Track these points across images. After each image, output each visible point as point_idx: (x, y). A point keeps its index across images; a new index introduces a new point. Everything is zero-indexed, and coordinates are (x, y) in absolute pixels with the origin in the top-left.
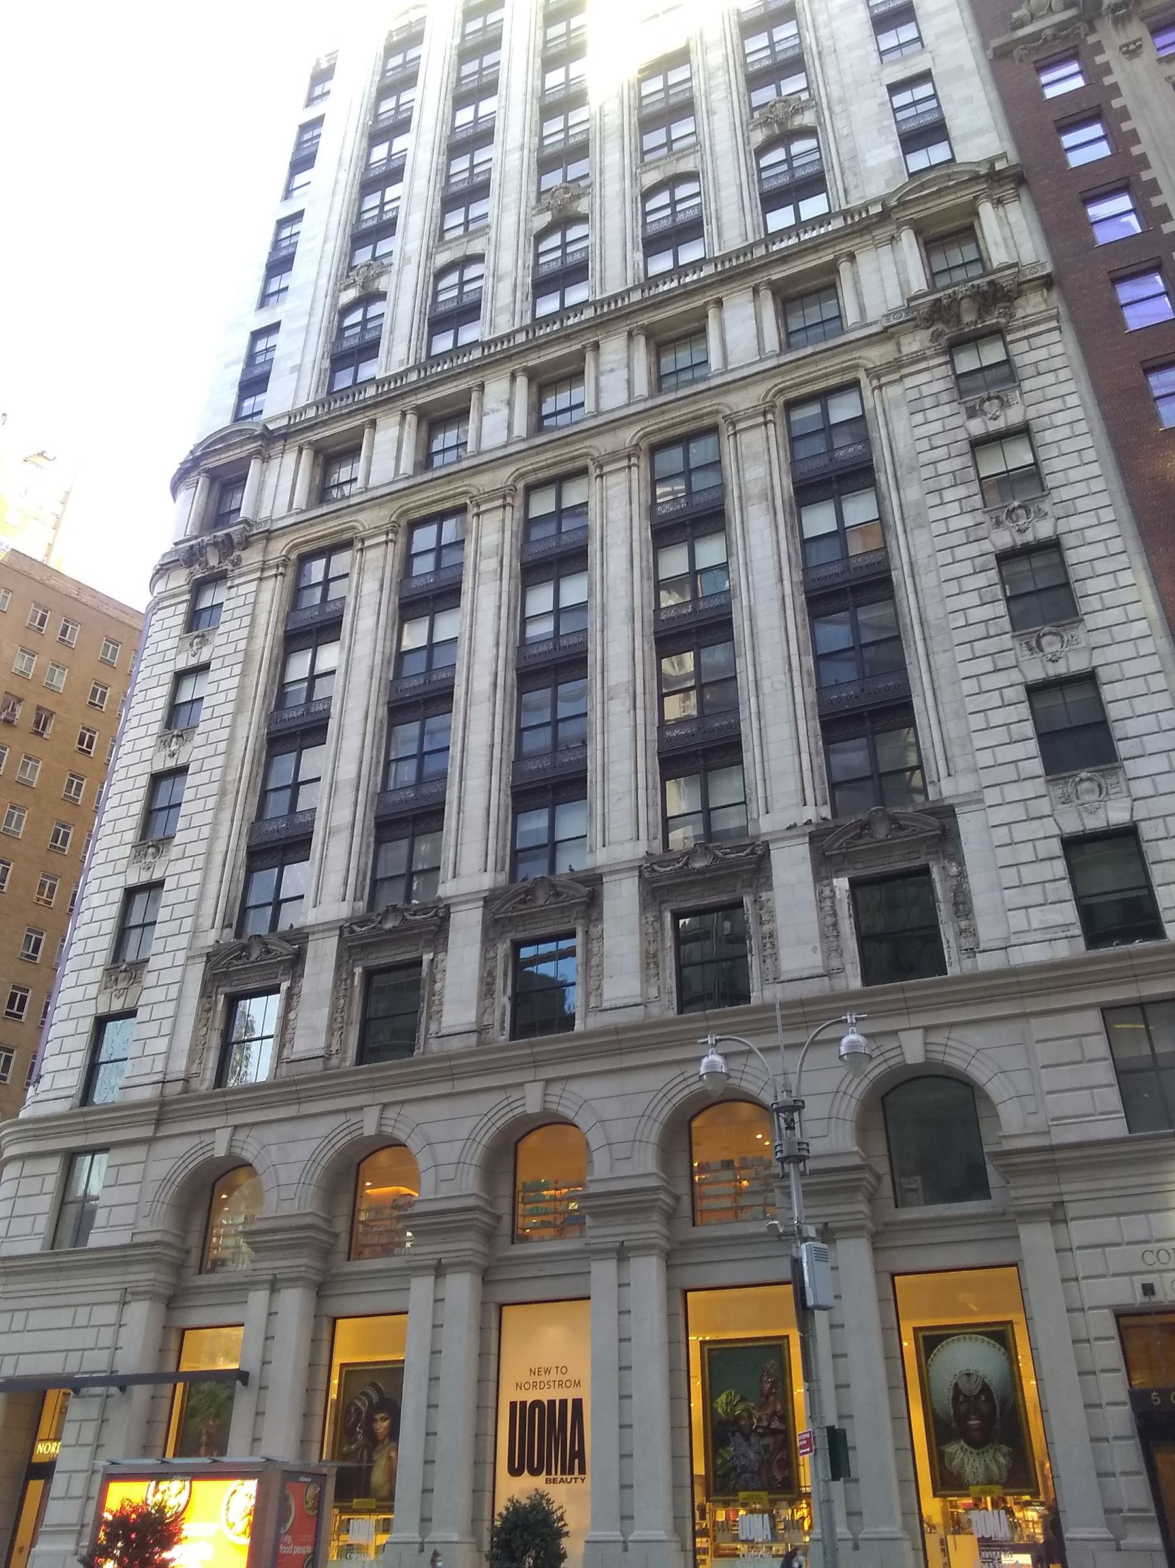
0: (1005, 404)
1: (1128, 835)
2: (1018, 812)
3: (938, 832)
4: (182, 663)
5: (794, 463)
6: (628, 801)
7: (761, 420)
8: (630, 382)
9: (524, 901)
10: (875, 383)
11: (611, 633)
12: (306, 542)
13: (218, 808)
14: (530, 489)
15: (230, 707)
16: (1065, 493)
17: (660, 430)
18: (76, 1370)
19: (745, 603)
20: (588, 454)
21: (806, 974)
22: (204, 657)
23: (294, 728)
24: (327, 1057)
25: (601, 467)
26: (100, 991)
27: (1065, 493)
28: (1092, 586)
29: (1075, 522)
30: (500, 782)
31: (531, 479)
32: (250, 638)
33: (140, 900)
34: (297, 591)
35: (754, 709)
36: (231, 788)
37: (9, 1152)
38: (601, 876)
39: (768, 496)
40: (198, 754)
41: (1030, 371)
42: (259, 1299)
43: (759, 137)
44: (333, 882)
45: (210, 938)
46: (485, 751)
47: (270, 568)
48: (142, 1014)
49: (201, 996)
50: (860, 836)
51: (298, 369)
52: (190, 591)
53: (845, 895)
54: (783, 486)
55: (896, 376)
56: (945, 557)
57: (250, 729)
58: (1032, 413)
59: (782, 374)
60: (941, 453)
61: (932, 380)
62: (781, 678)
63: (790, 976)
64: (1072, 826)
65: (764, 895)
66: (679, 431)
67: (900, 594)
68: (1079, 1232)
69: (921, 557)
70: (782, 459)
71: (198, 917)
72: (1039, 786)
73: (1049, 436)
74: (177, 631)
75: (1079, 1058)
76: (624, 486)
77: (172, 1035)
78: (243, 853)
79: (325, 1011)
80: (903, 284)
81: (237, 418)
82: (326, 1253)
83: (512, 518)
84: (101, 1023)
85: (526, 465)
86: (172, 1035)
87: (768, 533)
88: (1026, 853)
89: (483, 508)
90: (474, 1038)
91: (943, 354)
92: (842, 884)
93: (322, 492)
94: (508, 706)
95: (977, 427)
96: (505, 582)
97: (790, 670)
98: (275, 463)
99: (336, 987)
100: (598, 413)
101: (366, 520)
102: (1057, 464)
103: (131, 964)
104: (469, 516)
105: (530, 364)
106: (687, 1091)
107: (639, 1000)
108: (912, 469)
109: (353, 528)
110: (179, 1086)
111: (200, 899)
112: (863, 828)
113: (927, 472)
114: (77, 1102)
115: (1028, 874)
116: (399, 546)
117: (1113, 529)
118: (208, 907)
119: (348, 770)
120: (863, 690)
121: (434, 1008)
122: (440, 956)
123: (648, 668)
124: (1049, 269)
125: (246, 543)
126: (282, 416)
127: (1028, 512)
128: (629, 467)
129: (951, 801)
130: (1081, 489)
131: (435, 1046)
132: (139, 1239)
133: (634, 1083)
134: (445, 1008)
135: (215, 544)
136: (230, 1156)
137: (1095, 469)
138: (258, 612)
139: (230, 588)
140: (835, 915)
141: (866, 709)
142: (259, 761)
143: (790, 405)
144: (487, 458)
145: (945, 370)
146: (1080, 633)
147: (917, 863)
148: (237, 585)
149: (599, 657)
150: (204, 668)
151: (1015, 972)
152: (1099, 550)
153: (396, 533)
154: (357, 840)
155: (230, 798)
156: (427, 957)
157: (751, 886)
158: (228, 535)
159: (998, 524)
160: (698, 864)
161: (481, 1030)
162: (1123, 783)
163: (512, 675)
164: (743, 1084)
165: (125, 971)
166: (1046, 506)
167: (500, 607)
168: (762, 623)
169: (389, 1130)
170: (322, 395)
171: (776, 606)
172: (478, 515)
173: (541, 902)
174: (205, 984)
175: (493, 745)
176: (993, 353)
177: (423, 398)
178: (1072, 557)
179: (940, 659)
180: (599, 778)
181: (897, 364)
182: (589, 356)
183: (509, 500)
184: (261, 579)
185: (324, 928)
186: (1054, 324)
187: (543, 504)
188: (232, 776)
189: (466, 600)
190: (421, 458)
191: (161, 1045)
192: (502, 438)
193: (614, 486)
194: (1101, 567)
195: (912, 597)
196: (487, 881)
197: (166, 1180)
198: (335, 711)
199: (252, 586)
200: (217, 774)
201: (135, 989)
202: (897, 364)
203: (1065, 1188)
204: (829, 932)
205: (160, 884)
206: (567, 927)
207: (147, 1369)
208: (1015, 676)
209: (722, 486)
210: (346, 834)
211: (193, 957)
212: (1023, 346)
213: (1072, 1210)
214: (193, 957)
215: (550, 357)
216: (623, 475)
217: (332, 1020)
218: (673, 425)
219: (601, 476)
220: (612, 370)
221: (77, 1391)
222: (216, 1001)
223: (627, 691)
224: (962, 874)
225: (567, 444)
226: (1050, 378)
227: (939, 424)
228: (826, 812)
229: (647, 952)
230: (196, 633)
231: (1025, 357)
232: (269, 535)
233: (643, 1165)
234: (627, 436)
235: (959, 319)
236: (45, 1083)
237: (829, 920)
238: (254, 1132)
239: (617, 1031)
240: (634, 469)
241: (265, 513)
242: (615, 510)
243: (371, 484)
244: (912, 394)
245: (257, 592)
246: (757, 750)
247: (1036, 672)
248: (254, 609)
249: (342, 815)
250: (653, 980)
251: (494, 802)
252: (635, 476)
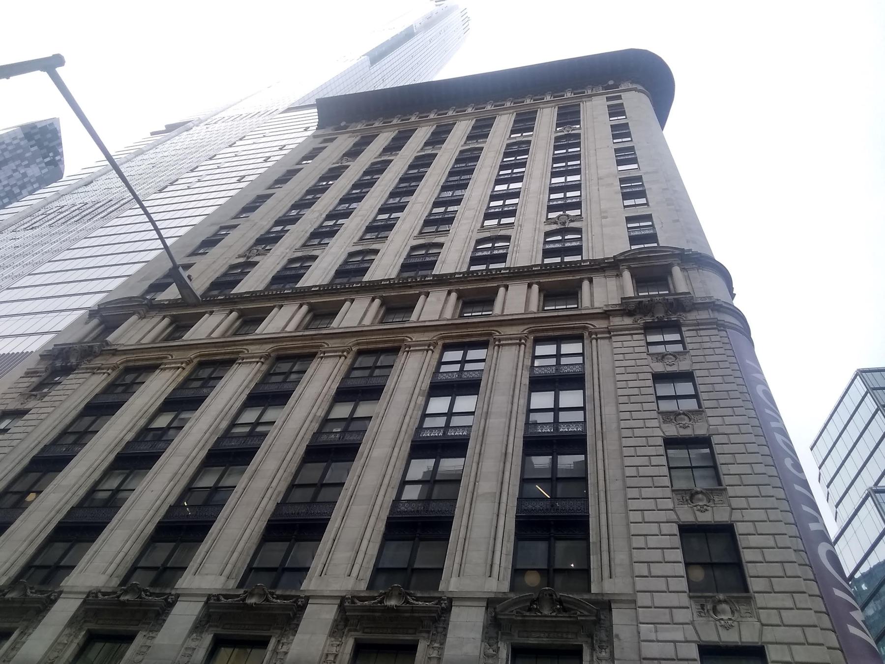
3: (594, 618)
100: (418, 321)
112: (533, 602)
120: (552, 506)
129: (611, 598)
157: (428, 632)
160: (392, 603)
172: (322, 358)
182: (422, 297)
228: (505, 587)
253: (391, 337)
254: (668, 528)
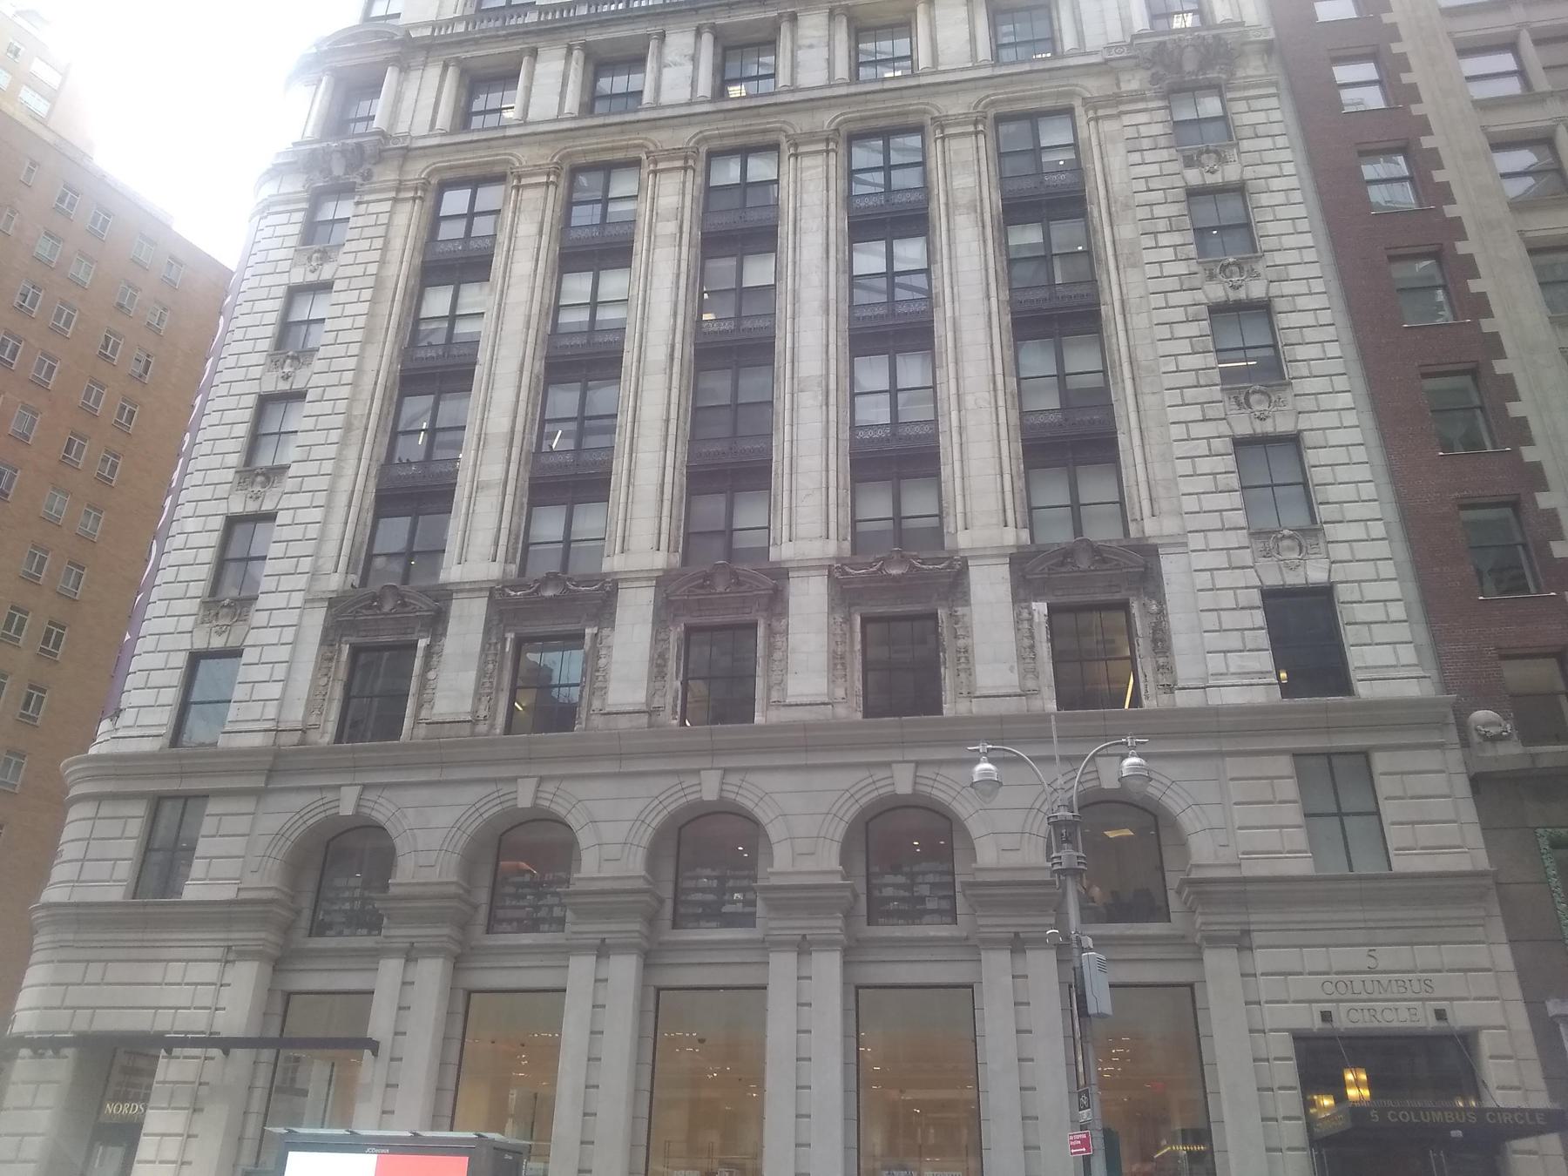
0: (1222, 160)
1: (1324, 594)
2: (1220, 560)
4: (299, 276)
5: (1002, 179)
6: (818, 498)
7: (971, 128)
8: (830, 63)
9: (702, 587)
10: (1091, 114)
11: (802, 321)
12: (451, 168)
13: (343, 443)
14: (712, 155)
15: (357, 336)
16: (1279, 258)
17: (862, 119)
18: (168, 1028)
19: (949, 314)
20: (781, 130)
21: (1002, 692)
22: (326, 273)
23: (434, 369)
24: (474, 722)
25: (796, 145)
26: (196, 625)
27: (1279, 258)
28: (1301, 352)
29: (1288, 288)
30: (676, 456)
31: (715, 144)
32: (382, 262)
33: (239, 530)
34: (436, 220)
35: (955, 423)
36: (358, 424)
37: (74, 792)
38: (787, 570)
39: (976, 207)
40: (316, 380)
41: (1248, 132)
42: (391, 969)
44: (482, 539)
45: (334, 582)
46: (660, 424)
47: (407, 189)
48: (249, 655)
49: (321, 644)
50: (1062, 564)
52: (308, 200)
53: (1044, 619)
54: (992, 200)
55: (1113, 111)
56: (1158, 301)
57: (380, 362)
58: (1249, 173)
59: (996, 87)
60: (1158, 196)
61: (1149, 122)
62: (985, 396)
63: (986, 692)
64: (1273, 579)
65: (960, 611)
66: (882, 123)
67: (1108, 330)
68: (1262, 959)
69: (1133, 295)
70: (992, 173)
71: (318, 558)
72: (1241, 538)
73: (1265, 199)
74: (293, 241)
75: (1270, 798)
76: (821, 170)
77: (286, 681)
78: (371, 496)
79: (472, 675)
80: (1125, 21)
81: (367, 18)
82: (464, 926)
83: (693, 183)
84: (196, 658)
85: (711, 129)
86: (286, 681)
87: (975, 246)
88: (1227, 600)
89: (661, 166)
90: (644, 719)
91: (1163, 98)
92: (1040, 608)
93: (464, 118)
94: (685, 382)
95: (1194, 177)
96: (685, 249)
97: (995, 390)
98: (415, 75)
99: (483, 649)
101: (524, 156)
102: (1272, 228)
103: (235, 600)
104: (644, 172)
105: (719, 22)
106: (875, 794)
107: (826, 700)
108: (1127, 206)
109: (508, 162)
110: (296, 737)
111: (320, 540)
113: (1142, 213)
114: (165, 741)
115: (1229, 620)
116: (560, 190)
117: (1322, 301)
118: (330, 548)
119: (499, 422)
121: (598, 685)
122: (606, 632)
123: (841, 366)
124: (1271, 35)
125: (380, 157)
126: (425, 25)
127: (1241, 269)
128: (828, 152)
130: (1293, 256)
131: (598, 721)
132: (244, 895)
133: (819, 780)
134: (612, 686)
135: (343, 152)
136: (357, 814)
137: (1308, 240)
138: (392, 234)
139: (358, 203)
140: (1032, 637)
141: (1070, 439)
142: (391, 398)
143: (1000, 119)
144: (669, 113)
145: (1161, 115)
146: (1287, 395)
147: (1117, 597)
148: (368, 202)
149: (789, 345)
150: (327, 286)
151: (1217, 711)
152: (1308, 319)
153: (558, 176)
154: (509, 499)
155: (356, 435)
156: (588, 631)
158: (359, 146)
159: (1211, 277)
161: (651, 712)
162: (1322, 545)
163: (690, 350)
164: (935, 792)
165: (229, 606)
166: (1259, 267)
167: (678, 276)
168: (966, 337)
169: (547, 804)
170: (471, 11)
171: (981, 322)
173: (720, 589)
174: (326, 632)
175: (667, 421)
176: (1211, 106)
177: (593, 36)
178: (1283, 321)
179: (1149, 401)
180: (787, 470)
181: (1116, 99)
182: (785, 28)
183: (691, 162)
184: (395, 200)
185: (473, 588)
186: (1272, 90)
187: (728, 173)
188: (359, 410)
189: (638, 261)
190: (586, 99)
191: (275, 690)
192: (684, 94)
193: (809, 168)
194: (1310, 335)
195: (1122, 334)
196: (659, 561)
197: (279, 834)
198: (483, 356)
199: (387, 206)
200: (342, 406)
201: (239, 629)
202: (1116, 99)
203: (1253, 918)
204: (1026, 653)
205: (270, 517)
206: (748, 618)
207: (253, 1034)
208: (1223, 428)
209: (926, 189)
210: (498, 491)
211: (313, 600)
212: (1242, 106)
213: (1258, 938)
214: (313, 600)
215: (746, 18)
216: (820, 160)
217: (479, 684)
218: (876, 117)
219: (796, 156)
220: (811, 46)
221: (169, 1051)
222: (340, 650)
223: (820, 384)
224: (1162, 613)
225: (759, 115)
226: (1268, 143)
227: (1156, 166)
228: (1025, 536)
229: (835, 652)
230: (316, 247)
231: (1245, 118)
232: (407, 154)
233: (824, 862)
234: (826, 120)
235: (1180, 66)
236: (127, 718)
237: (1027, 642)
238: (386, 793)
239: (805, 727)
240: (832, 155)
241: (402, 128)
242: (809, 196)
243: (531, 116)
244: (1130, 132)
245: (391, 213)
246: (957, 465)
247: (1243, 427)
248: (387, 231)
249: (493, 470)
250: (840, 681)
251: (668, 479)
252: (832, 161)
253: (758, 123)
254: (1218, 445)
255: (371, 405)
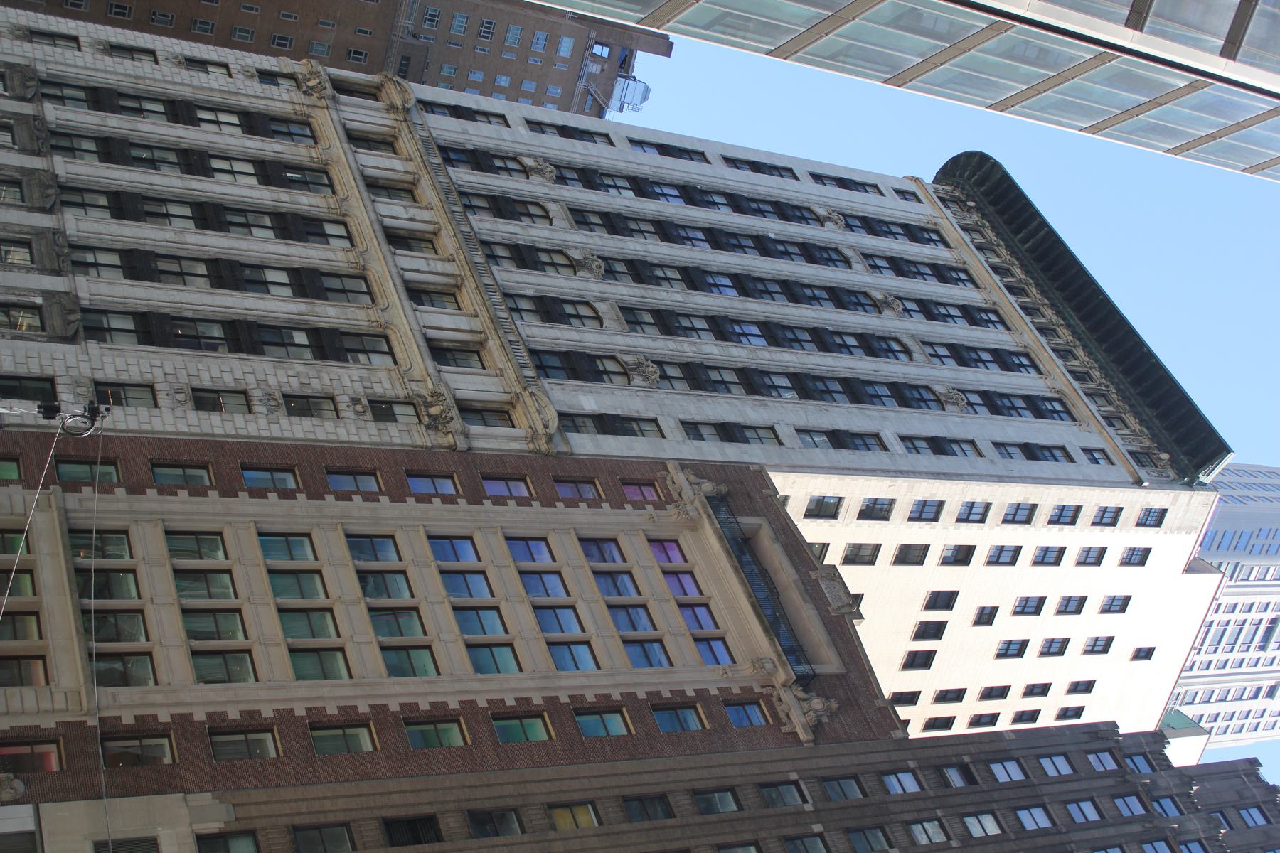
8: (417, 271)
32: (248, 96)
43: (628, 358)
45: (41, 67)
51: (465, 132)
64: (58, 380)
92: (39, 301)
98: (386, 115)
179: (180, 358)
188: (147, 82)
255: (150, 86)
